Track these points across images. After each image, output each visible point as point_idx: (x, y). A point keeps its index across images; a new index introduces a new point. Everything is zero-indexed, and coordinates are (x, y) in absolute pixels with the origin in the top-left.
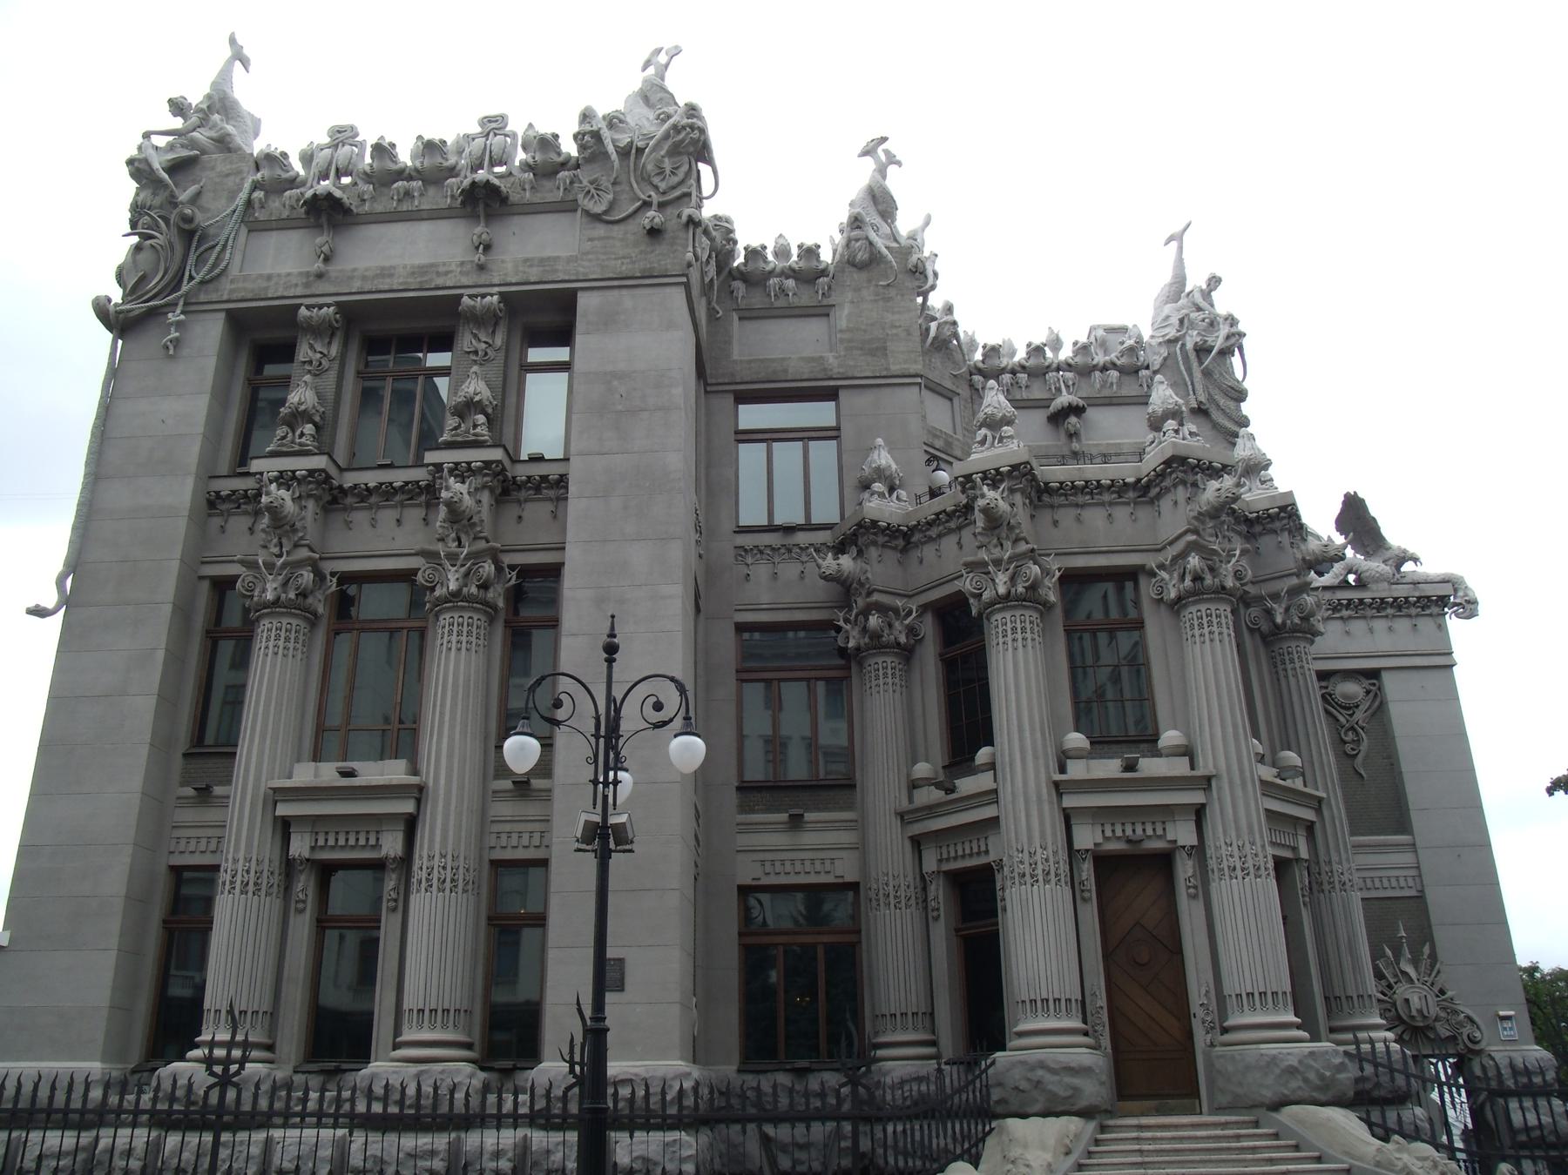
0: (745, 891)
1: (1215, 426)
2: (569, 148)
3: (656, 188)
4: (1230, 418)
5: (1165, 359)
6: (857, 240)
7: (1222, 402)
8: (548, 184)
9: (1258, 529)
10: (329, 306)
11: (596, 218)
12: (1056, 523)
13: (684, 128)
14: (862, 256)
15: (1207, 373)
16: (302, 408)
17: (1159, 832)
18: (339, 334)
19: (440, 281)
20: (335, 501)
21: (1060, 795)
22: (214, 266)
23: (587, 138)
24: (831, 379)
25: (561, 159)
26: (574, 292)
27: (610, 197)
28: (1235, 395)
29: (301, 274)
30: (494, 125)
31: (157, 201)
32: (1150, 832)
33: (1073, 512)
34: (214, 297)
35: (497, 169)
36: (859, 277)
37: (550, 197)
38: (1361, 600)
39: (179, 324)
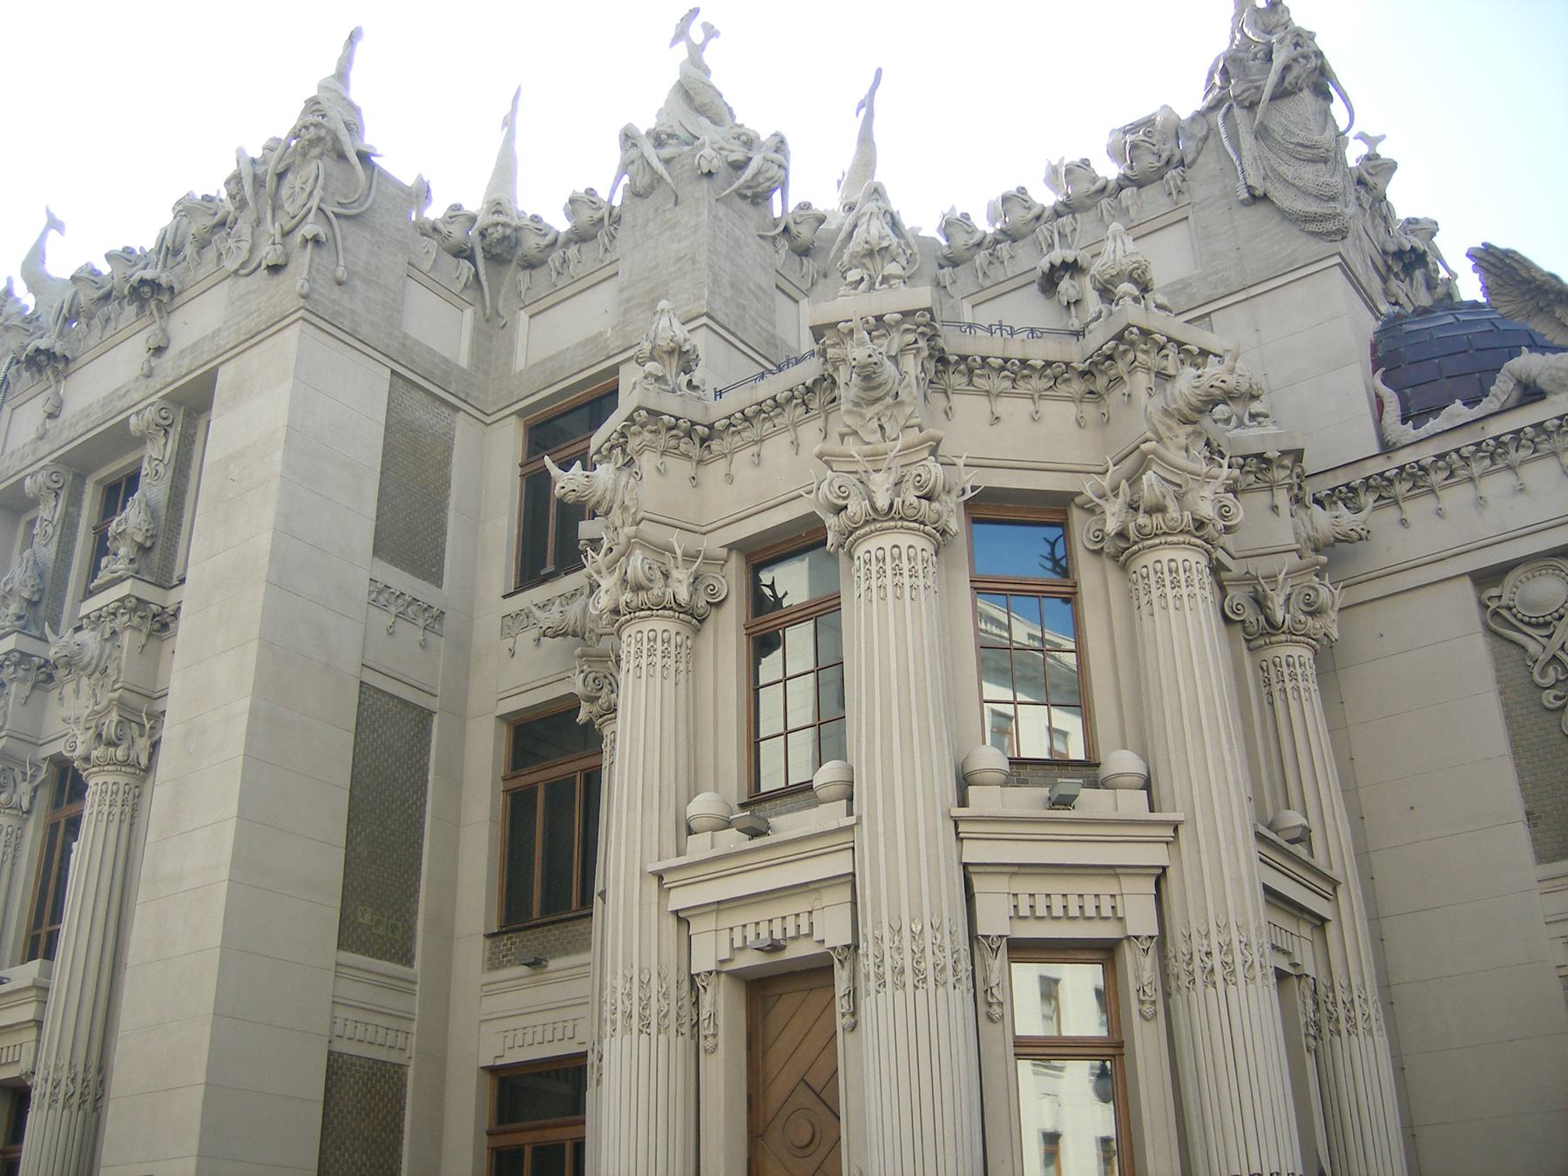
0: (492, 1070)
1: (1288, 216)
4: (1307, 194)
5: (1206, 138)
6: (632, 162)
7: (1289, 171)
9: (1101, 382)
12: (729, 478)
14: (643, 181)
15: (1262, 133)
17: (804, 930)
18: (62, 494)
19: (120, 405)
20: (50, 678)
21: (664, 890)
24: (609, 358)
28: (1309, 153)
32: (791, 932)
33: (755, 449)
36: (644, 207)
38: (1538, 426)
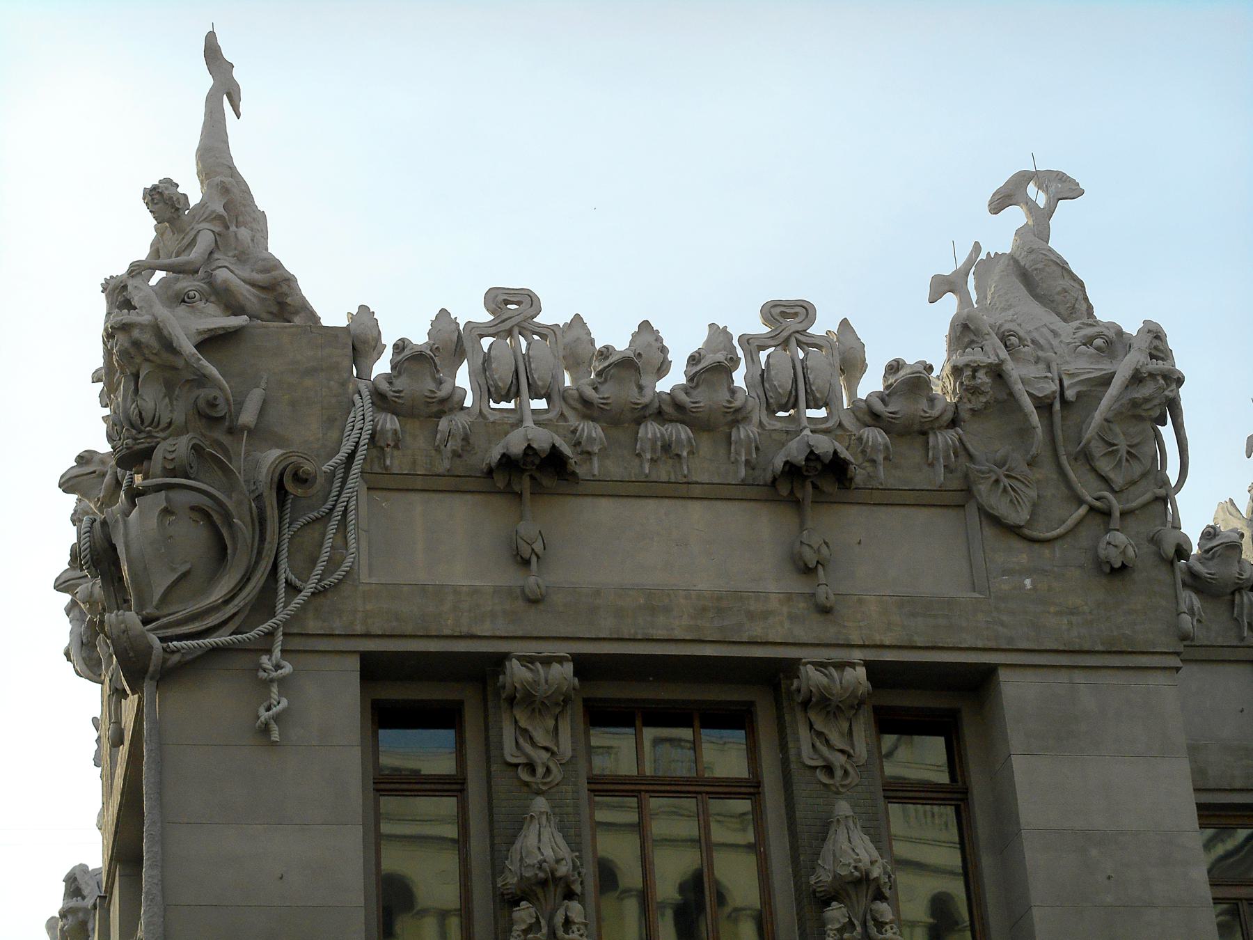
2: (943, 387)
3: (1105, 480)
8: (911, 454)
10: (560, 660)
11: (1014, 531)
13: (1152, 375)
16: (563, 870)
19: (756, 630)
22: (333, 564)
23: (982, 377)
25: (935, 413)
26: (988, 673)
27: (1033, 493)
29: (497, 590)
30: (791, 324)
31: (179, 417)
34: (338, 626)
35: (812, 413)
37: (920, 479)
39: (282, 681)
